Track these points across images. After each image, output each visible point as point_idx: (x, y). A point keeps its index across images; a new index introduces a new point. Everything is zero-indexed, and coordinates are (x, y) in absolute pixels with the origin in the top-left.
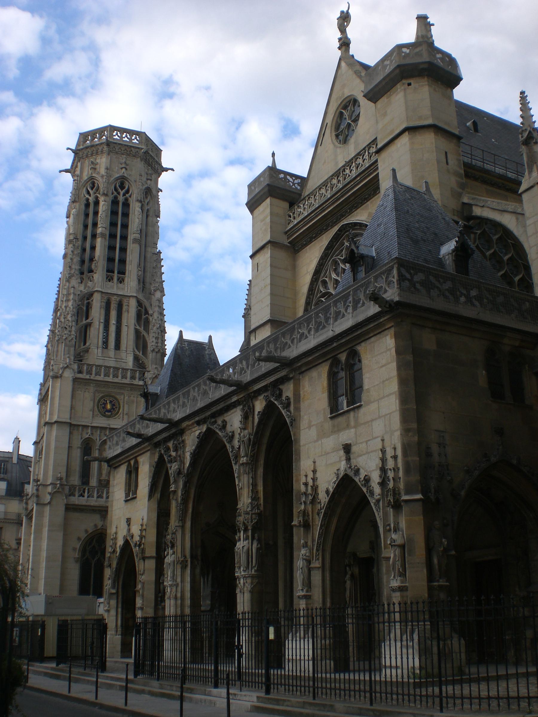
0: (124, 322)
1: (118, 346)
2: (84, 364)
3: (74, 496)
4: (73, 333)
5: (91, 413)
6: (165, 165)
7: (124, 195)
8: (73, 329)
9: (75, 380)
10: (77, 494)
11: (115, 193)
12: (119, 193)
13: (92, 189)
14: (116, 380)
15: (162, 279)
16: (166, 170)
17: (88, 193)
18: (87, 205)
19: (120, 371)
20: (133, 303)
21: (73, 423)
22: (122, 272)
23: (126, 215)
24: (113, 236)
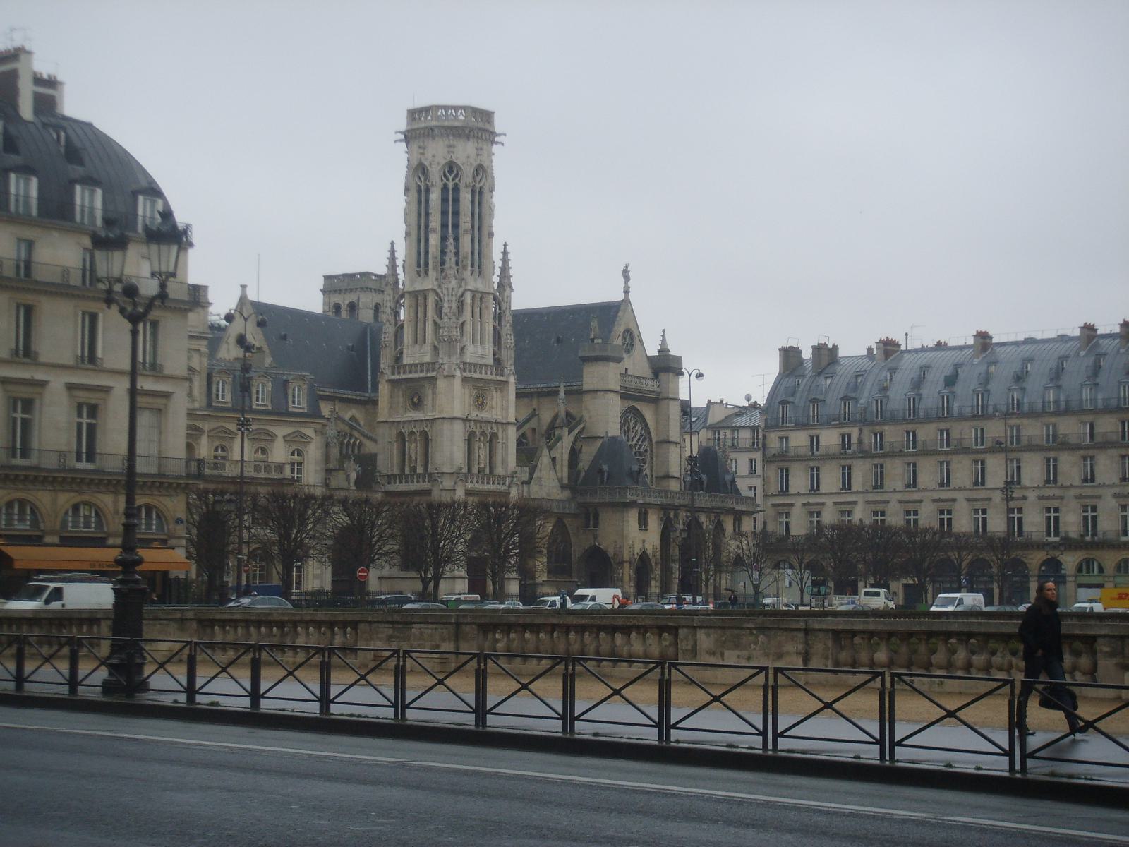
4: (459, 334)
14: (485, 377)
16: (497, 143)
17: (445, 175)
18: (445, 189)
22: (479, 267)
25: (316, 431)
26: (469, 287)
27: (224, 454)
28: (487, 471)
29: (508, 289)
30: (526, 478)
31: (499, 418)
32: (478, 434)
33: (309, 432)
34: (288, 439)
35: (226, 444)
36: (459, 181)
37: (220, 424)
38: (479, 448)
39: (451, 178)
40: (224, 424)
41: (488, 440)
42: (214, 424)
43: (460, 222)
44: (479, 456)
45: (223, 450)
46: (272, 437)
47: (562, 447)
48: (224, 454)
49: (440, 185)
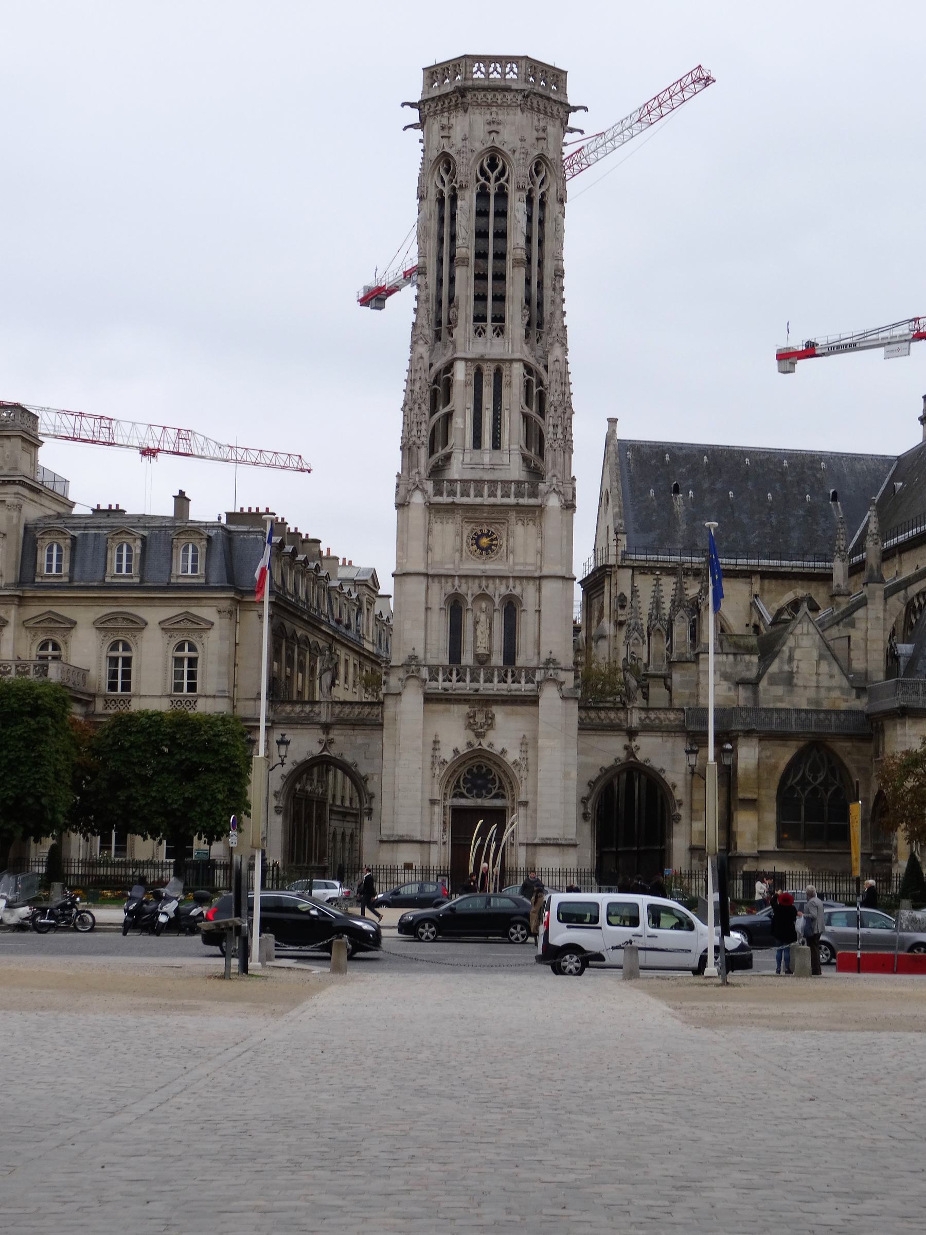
0: (505, 401)
1: (496, 444)
2: (443, 481)
3: (437, 680)
4: (424, 433)
5: (457, 554)
6: (572, 101)
7: (497, 179)
8: (424, 426)
9: (431, 507)
10: (441, 678)
11: (483, 180)
12: (488, 179)
13: (447, 171)
14: (492, 500)
15: (563, 322)
16: (575, 109)
18: (441, 201)
19: (499, 487)
20: (518, 369)
21: (431, 572)
22: (499, 319)
23: (502, 214)
24: (481, 255)
25: (219, 612)
26: (459, 354)
27: (56, 653)
28: (497, 660)
29: (557, 351)
30: (752, 674)
31: (531, 571)
32: (470, 599)
33: (207, 612)
34: (166, 625)
35: (59, 639)
36: (456, 183)
37: (48, 609)
38: (476, 623)
39: (446, 179)
40: (56, 609)
41: (497, 607)
42: (34, 611)
43: (508, 249)
44: (476, 637)
45: (56, 647)
46: (139, 625)
47: (867, 619)
48: (56, 653)
49: (433, 195)
